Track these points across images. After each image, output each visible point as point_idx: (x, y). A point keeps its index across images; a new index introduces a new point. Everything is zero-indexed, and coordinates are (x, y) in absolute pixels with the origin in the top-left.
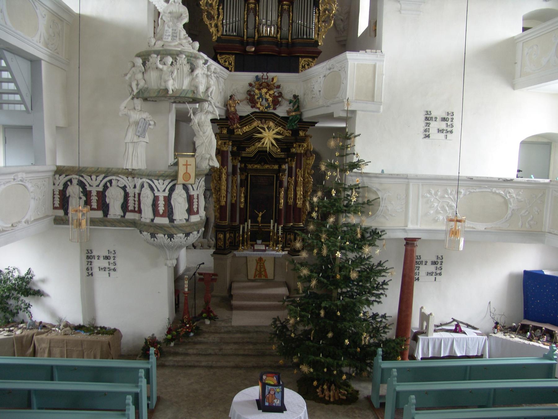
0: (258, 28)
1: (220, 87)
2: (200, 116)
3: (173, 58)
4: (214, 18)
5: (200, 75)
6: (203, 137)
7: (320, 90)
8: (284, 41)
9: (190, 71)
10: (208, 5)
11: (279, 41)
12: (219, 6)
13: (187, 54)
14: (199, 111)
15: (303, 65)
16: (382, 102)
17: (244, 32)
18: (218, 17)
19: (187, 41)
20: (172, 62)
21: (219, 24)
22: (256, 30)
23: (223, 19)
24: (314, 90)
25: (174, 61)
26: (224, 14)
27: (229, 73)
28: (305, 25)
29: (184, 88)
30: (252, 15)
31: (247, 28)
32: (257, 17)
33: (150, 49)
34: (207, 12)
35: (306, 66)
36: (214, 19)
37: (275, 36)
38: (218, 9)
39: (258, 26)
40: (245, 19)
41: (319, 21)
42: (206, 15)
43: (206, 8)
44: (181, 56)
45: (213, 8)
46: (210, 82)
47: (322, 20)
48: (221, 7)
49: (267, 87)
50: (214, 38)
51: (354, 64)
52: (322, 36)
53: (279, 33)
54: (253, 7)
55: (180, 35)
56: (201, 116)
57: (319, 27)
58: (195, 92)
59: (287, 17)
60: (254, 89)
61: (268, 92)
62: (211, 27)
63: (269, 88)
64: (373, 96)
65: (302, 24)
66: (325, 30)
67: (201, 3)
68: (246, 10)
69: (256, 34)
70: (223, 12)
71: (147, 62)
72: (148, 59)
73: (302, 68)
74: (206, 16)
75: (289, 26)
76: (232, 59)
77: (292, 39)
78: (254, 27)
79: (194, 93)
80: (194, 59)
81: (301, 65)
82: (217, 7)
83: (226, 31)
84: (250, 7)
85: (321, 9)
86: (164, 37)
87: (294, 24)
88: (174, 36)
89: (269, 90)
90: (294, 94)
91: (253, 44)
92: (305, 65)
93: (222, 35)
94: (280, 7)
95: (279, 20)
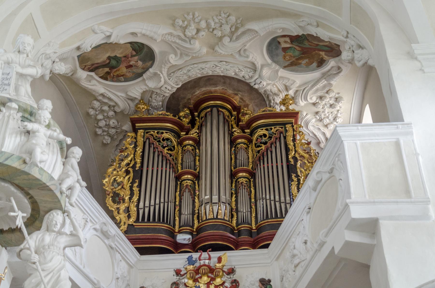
0: (198, 213)
1: (116, 270)
2: (40, 236)
6: (42, 273)
7: (305, 238)
11: (234, 228)
12: (133, 183)
13: (21, 104)
14: (43, 230)
16: (429, 198)
17: (174, 220)
18: (130, 199)
21: (133, 209)
23: (139, 200)
24: (295, 252)
27: (139, 257)
29: (3, 150)
30: (187, 196)
31: (180, 214)
34: (114, 193)
38: (131, 188)
39: (198, 210)
40: (177, 203)
42: (112, 197)
43: (112, 187)
44: (9, 104)
45: (122, 187)
46: (68, 171)
48: (136, 185)
49: (210, 275)
51: (356, 143)
53: (235, 218)
54: (189, 184)
56: (43, 236)
58: (28, 160)
59: (247, 194)
60: (186, 280)
61: (211, 284)
62: (118, 213)
63: (212, 276)
64: (408, 192)
67: (104, 182)
68: (178, 190)
69: (196, 222)
70: (140, 191)
74: (111, 198)
75: (251, 207)
79: (25, 162)
84: (185, 185)
85: (300, 176)
88: (5, 85)
89: (213, 279)
90: (261, 277)
91: (191, 233)
94: (234, 182)
95: (234, 199)
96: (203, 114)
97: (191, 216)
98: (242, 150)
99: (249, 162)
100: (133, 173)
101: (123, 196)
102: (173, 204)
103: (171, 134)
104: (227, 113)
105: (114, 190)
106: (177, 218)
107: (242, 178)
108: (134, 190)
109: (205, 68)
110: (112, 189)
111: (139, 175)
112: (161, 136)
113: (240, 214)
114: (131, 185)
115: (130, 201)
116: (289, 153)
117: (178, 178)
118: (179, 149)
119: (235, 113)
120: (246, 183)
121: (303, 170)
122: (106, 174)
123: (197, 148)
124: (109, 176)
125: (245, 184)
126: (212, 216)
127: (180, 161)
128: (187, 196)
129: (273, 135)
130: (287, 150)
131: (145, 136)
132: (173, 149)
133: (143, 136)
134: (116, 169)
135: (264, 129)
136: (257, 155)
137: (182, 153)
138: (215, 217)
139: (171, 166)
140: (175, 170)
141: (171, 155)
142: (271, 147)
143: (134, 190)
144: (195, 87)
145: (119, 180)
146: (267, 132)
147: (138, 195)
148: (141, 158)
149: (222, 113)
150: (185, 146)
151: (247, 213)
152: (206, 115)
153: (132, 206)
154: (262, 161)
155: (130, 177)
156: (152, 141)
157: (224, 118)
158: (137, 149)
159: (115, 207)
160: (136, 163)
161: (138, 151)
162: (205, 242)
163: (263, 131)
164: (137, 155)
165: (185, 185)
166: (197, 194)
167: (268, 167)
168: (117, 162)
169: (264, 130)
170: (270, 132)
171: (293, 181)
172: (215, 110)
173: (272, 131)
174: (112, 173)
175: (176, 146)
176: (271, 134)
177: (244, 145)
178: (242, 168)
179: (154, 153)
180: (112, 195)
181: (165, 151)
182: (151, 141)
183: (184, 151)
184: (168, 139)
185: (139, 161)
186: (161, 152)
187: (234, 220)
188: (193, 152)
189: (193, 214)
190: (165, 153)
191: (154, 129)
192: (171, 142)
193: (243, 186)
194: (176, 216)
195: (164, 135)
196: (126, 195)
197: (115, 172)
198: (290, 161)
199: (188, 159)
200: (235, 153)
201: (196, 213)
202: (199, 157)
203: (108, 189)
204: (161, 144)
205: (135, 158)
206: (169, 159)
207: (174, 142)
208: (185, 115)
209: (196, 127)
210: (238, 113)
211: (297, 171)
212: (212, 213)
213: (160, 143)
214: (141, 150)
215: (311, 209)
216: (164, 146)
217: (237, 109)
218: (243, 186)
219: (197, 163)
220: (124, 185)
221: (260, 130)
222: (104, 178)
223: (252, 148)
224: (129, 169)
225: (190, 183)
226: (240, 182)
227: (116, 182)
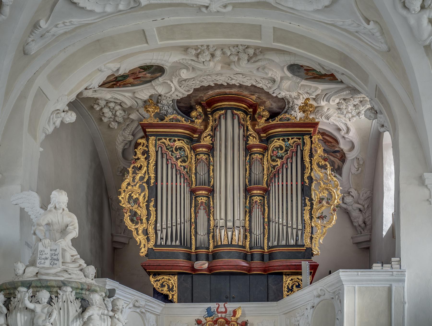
0: (213, 232)
3: (50, 292)
4: (141, 220)
5: (96, 317)
8: (257, 251)
9: (80, 310)
10: (132, 201)
11: (247, 252)
12: (148, 202)
15: (290, 286)
18: (148, 219)
19: (77, 265)
20: (51, 298)
21: (151, 230)
22: (211, 235)
25: (53, 296)
26: (156, 214)
28: (290, 225)
30: (202, 213)
32: (211, 216)
33: (17, 280)
34: (131, 211)
35: (294, 287)
36: (142, 223)
37: (240, 244)
38: (148, 207)
39: (213, 229)
40: (193, 220)
41: (311, 218)
43: (129, 206)
45: (139, 206)
47: (318, 215)
48: (152, 204)
50: (143, 251)
52: (317, 240)
53: (248, 240)
54: (204, 201)
55: (63, 257)
57: (312, 227)
59: (260, 213)
65: (285, 224)
66: (323, 231)
67: (120, 198)
68: (193, 205)
70: (156, 211)
71: (12, 299)
72: (14, 293)
73: (288, 292)
74: (128, 218)
75: (264, 228)
76: (173, 282)
77: (269, 247)
78: (206, 232)
80: (87, 293)
81: (286, 287)
82: (145, 203)
83: (162, 238)
84: (200, 201)
86: (38, 261)
87: (271, 223)
92: (292, 286)
93: (156, 245)
94: (248, 198)
95: (247, 219)
96: (217, 116)
97: (206, 236)
98: (257, 161)
99: (263, 174)
100: (148, 190)
101: (140, 216)
102: (189, 223)
103: (183, 140)
104: (242, 115)
105: (131, 208)
106: (193, 237)
107: (257, 197)
108: (151, 211)
109: (220, 80)
110: (129, 208)
111: (154, 193)
112: (174, 145)
113: (253, 235)
114: (147, 203)
115: (148, 223)
116: (305, 172)
117: (193, 192)
118: (192, 155)
119: (251, 110)
120: (261, 203)
121: (317, 193)
122: (121, 188)
123: (210, 156)
124: (124, 191)
125: (259, 203)
126: (225, 242)
127: (194, 171)
128: (202, 213)
129: (290, 148)
130: (303, 168)
131: (157, 145)
132: (186, 160)
133: (155, 144)
134: (131, 183)
135: (281, 140)
136: (272, 171)
137: (195, 161)
138: (230, 243)
139: (186, 181)
140: (190, 184)
141: (185, 168)
142: (287, 163)
143: (151, 210)
144: (209, 90)
145: (135, 197)
146: (284, 143)
147: (155, 216)
148: (154, 172)
149: (236, 116)
150: (199, 154)
151: (260, 235)
152: (220, 117)
153: (150, 228)
154: (277, 176)
155: (145, 193)
156: (165, 151)
157: (239, 123)
158: (150, 160)
159: (133, 227)
160: (149, 178)
161: (151, 164)
162: (220, 269)
163: (279, 141)
164: (150, 168)
165: (200, 201)
166: (212, 211)
167: (283, 185)
168: (130, 175)
169: (281, 141)
170: (287, 144)
171: (306, 205)
172: (229, 112)
173: (289, 142)
174: (127, 188)
175: (189, 155)
176: (288, 147)
177: (259, 155)
178: (256, 186)
179: (167, 165)
180: (130, 214)
181: (179, 164)
182: (163, 152)
183: (197, 161)
184: (180, 148)
185: (153, 176)
186: (175, 164)
187: (247, 242)
188: (207, 161)
189: (209, 233)
190: (179, 166)
191: (166, 135)
192: (184, 151)
193: (257, 206)
194: (192, 235)
195: (177, 144)
196: (143, 215)
197: (129, 187)
198: (305, 182)
199: (202, 171)
200: (250, 163)
201: (212, 232)
202: (213, 166)
203: (125, 207)
204: (175, 156)
205: (149, 171)
206: (183, 173)
207: (188, 150)
208: (197, 116)
209: (210, 128)
210: (255, 112)
211: (311, 194)
212: (226, 238)
213: (173, 154)
214: (154, 162)
215: (314, 307)
216: (178, 157)
217: (251, 106)
218: (257, 206)
219: (211, 174)
220: (140, 203)
221: (277, 139)
222: (120, 194)
223: (267, 157)
224: (144, 184)
225: (205, 199)
226: (254, 200)
227: (132, 200)
